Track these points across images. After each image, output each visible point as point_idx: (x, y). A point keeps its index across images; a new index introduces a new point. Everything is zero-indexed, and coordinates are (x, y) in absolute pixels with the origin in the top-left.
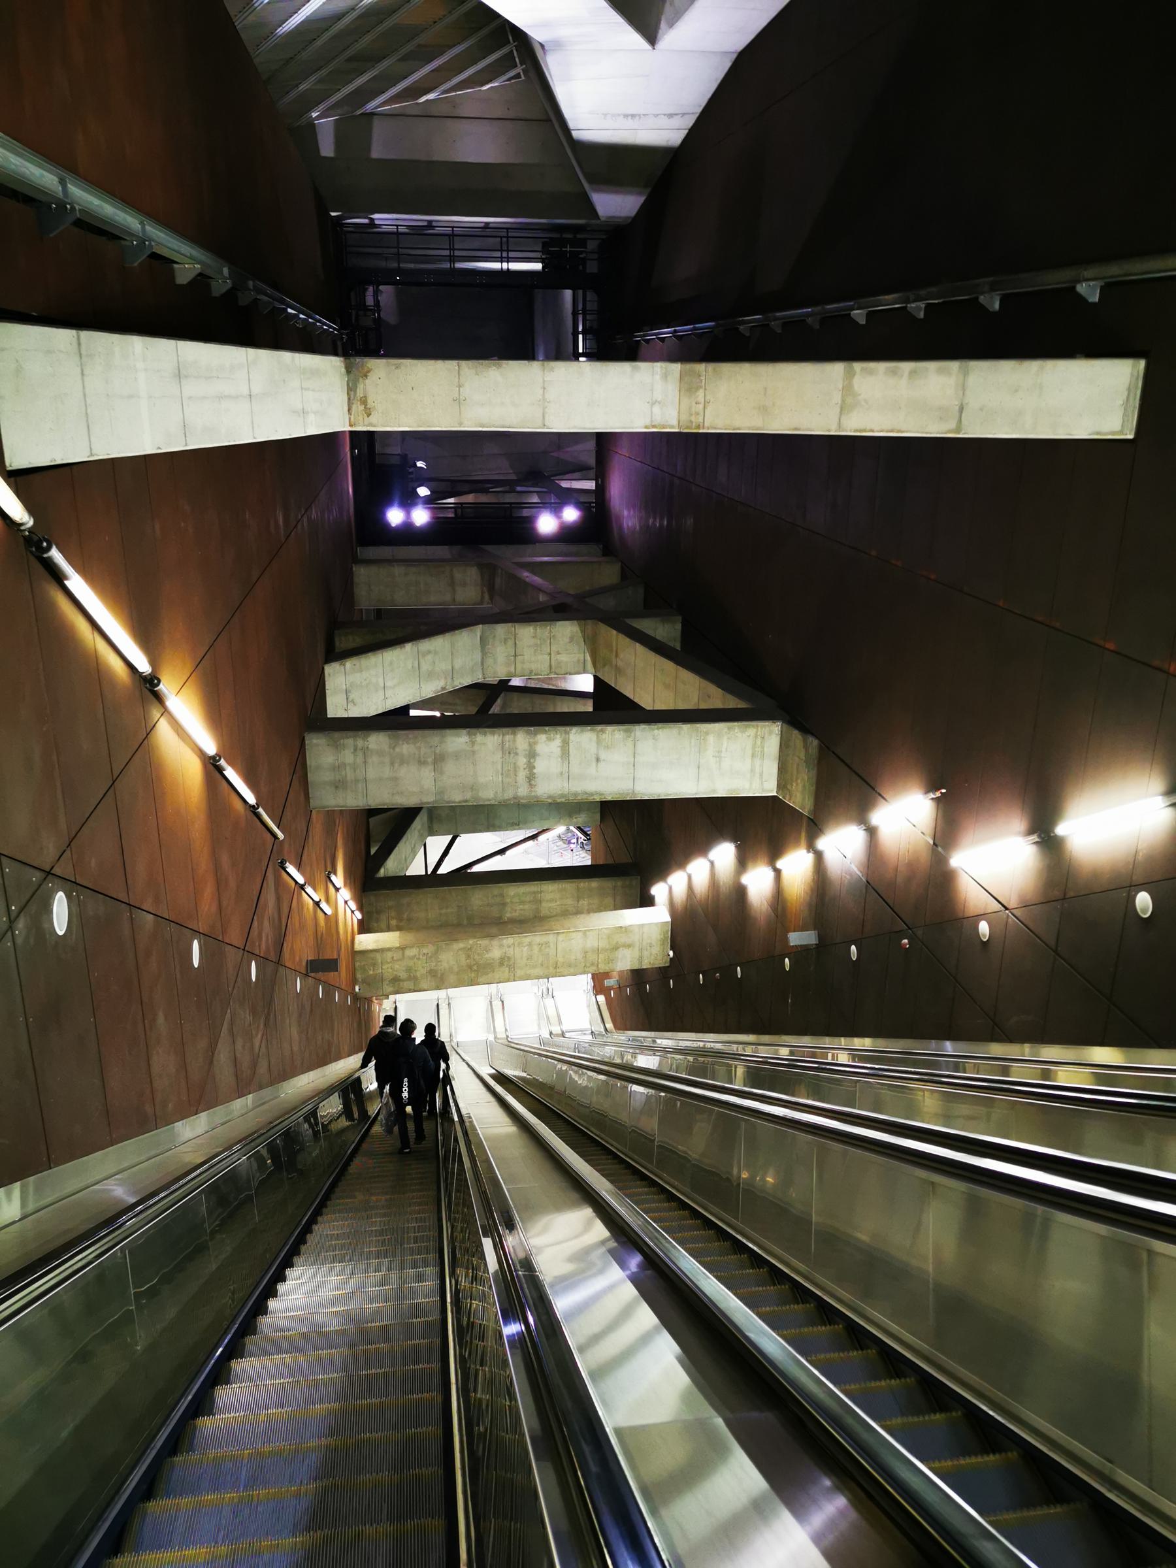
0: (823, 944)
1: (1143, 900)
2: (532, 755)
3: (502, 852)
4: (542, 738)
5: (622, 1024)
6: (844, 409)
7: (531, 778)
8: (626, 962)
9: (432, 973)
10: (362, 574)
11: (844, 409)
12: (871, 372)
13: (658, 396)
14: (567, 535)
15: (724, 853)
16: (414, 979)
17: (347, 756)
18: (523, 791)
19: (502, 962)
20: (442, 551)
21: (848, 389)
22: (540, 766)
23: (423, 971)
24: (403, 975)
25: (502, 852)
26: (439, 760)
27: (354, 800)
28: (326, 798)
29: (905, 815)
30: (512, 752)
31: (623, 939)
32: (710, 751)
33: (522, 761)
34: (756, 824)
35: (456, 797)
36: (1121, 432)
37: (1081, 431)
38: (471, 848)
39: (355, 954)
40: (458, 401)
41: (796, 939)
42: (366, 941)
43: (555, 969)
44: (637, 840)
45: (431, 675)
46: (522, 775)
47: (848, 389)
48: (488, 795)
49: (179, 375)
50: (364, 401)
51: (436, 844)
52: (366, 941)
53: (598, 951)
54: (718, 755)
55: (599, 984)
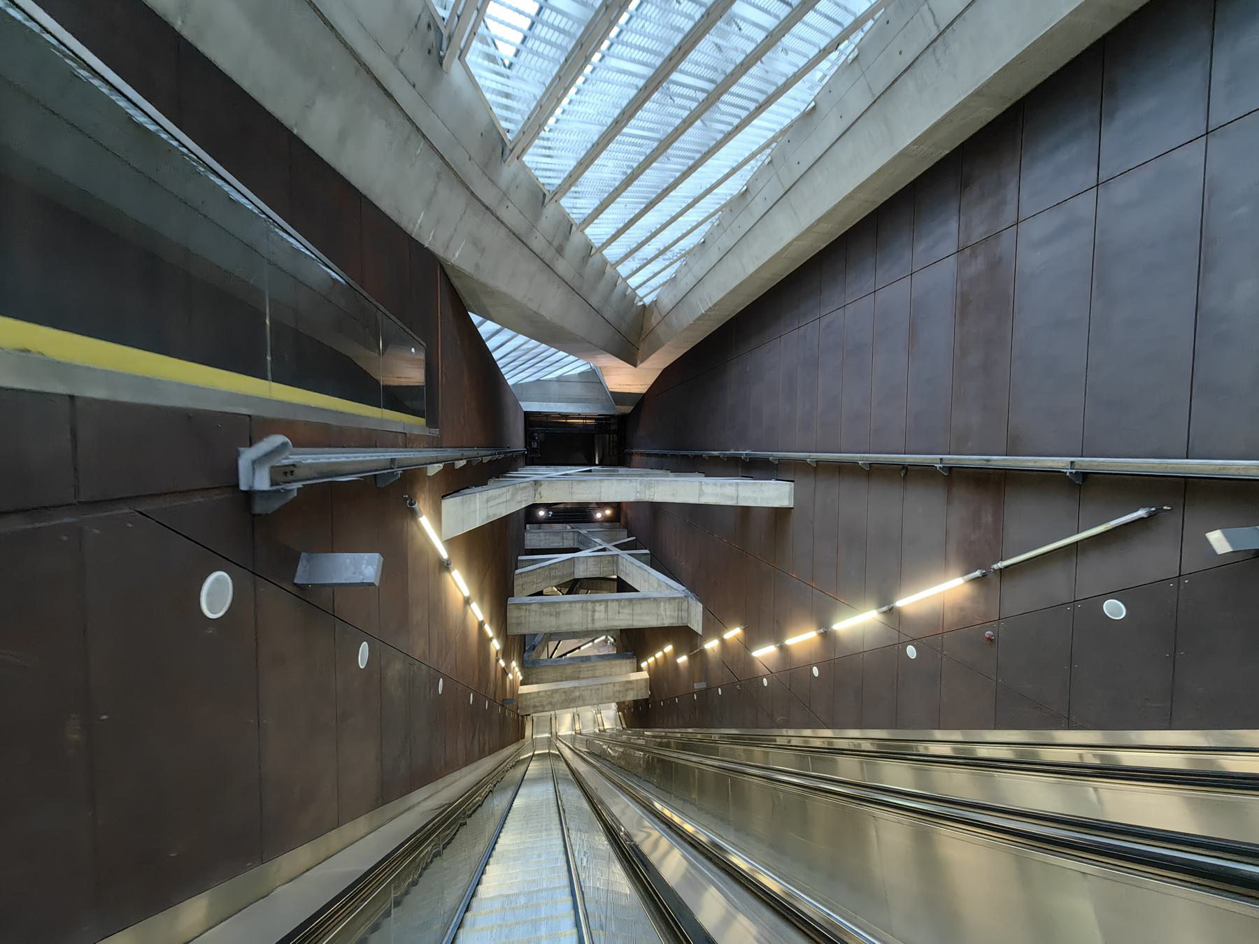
1: (816, 671)
2: (594, 611)
5: (630, 726)
6: (700, 495)
7: (593, 620)
8: (630, 697)
9: (551, 703)
10: (528, 536)
11: (700, 495)
12: (707, 484)
15: (669, 648)
16: (543, 706)
17: (523, 613)
18: (590, 626)
20: (558, 527)
21: (701, 490)
22: (597, 615)
26: (558, 614)
29: (734, 633)
30: (587, 609)
31: (630, 686)
34: (683, 636)
35: (564, 629)
37: (777, 505)
38: (566, 645)
39: (516, 697)
41: (697, 686)
42: (524, 690)
44: (633, 643)
45: (554, 577)
47: (701, 490)
48: (577, 628)
49: (488, 501)
51: (552, 645)
52: (524, 690)
55: (621, 707)
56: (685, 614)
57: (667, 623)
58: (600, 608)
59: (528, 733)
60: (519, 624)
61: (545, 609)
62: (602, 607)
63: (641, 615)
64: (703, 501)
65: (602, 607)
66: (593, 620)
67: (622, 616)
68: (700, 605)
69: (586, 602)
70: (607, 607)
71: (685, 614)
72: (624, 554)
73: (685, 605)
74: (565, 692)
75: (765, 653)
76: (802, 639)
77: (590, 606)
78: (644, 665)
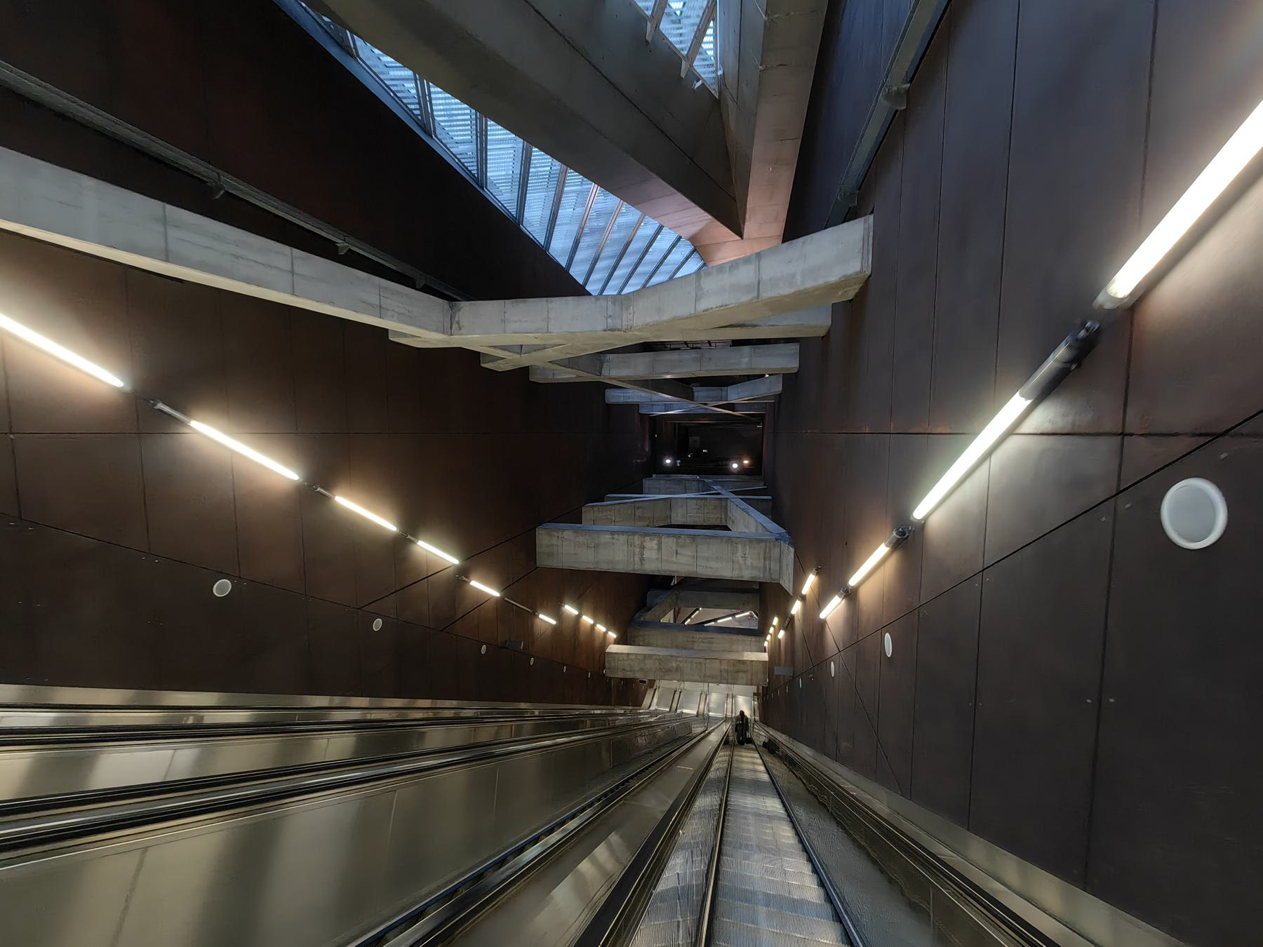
0: (794, 678)
2: (643, 547)
3: (715, 620)
4: (648, 539)
7: (642, 559)
11: (697, 299)
13: (610, 313)
14: (744, 471)
17: (554, 541)
19: (678, 669)
22: (647, 554)
23: (637, 668)
24: (628, 668)
25: (715, 620)
26: (596, 547)
27: (554, 563)
28: (543, 561)
31: (742, 667)
32: (739, 554)
33: (637, 550)
36: (861, 271)
40: (504, 321)
43: (705, 679)
45: (641, 519)
46: (637, 558)
48: (620, 568)
50: (458, 323)
53: (727, 672)
54: (744, 557)
56: (775, 566)
57: (747, 575)
58: (651, 544)
59: (646, 702)
60: (551, 555)
61: (581, 539)
62: (654, 544)
63: (708, 559)
64: (702, 306)
65: (654, 544)
66: (642, 559)
67: (682, 559)
68: (792, 550)
69: (634, 533)
70: (659, 544)
71: (775, 566)
72: (737, 500)
73: (777, 550)
74: (660, 660)
75: (833, 609)
76: (874, 566)
77: (637, 540)
78: (766, 644)
